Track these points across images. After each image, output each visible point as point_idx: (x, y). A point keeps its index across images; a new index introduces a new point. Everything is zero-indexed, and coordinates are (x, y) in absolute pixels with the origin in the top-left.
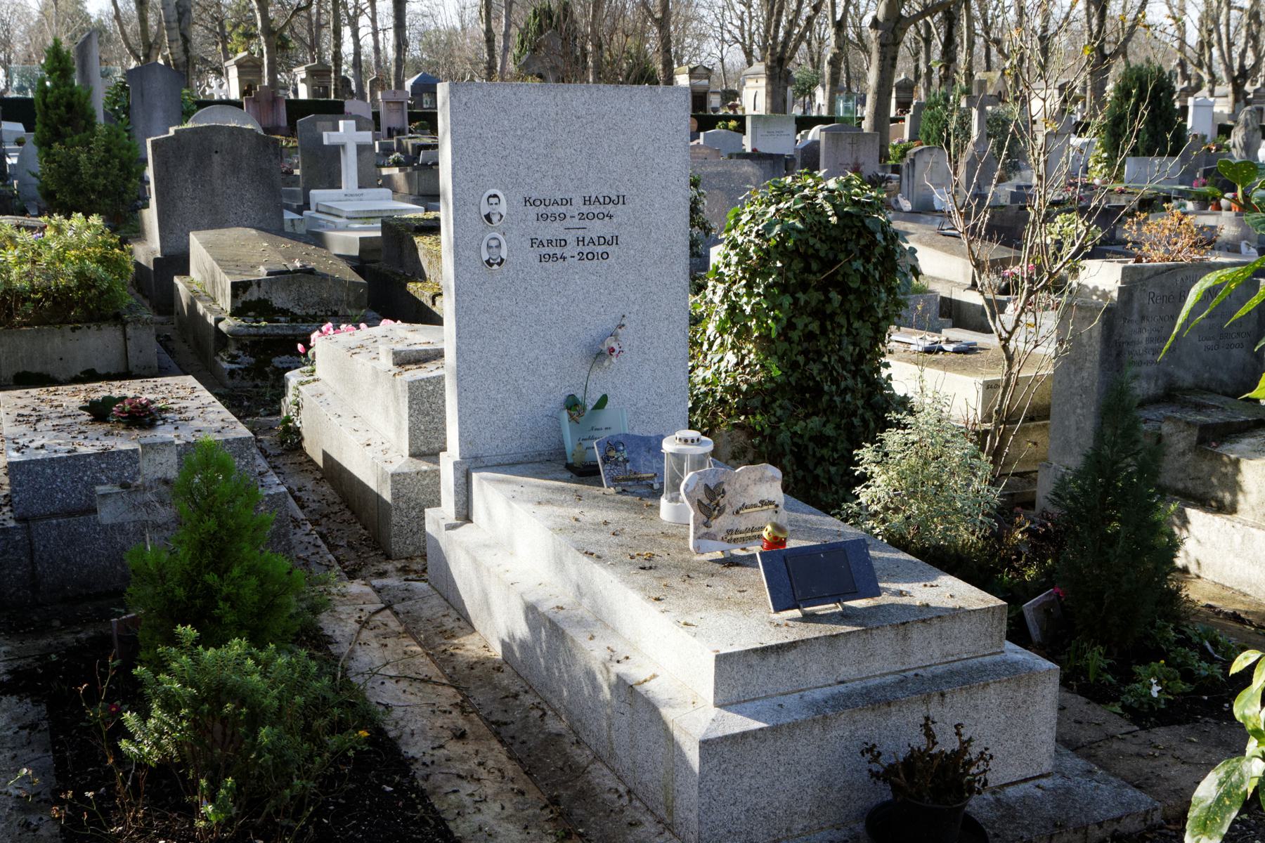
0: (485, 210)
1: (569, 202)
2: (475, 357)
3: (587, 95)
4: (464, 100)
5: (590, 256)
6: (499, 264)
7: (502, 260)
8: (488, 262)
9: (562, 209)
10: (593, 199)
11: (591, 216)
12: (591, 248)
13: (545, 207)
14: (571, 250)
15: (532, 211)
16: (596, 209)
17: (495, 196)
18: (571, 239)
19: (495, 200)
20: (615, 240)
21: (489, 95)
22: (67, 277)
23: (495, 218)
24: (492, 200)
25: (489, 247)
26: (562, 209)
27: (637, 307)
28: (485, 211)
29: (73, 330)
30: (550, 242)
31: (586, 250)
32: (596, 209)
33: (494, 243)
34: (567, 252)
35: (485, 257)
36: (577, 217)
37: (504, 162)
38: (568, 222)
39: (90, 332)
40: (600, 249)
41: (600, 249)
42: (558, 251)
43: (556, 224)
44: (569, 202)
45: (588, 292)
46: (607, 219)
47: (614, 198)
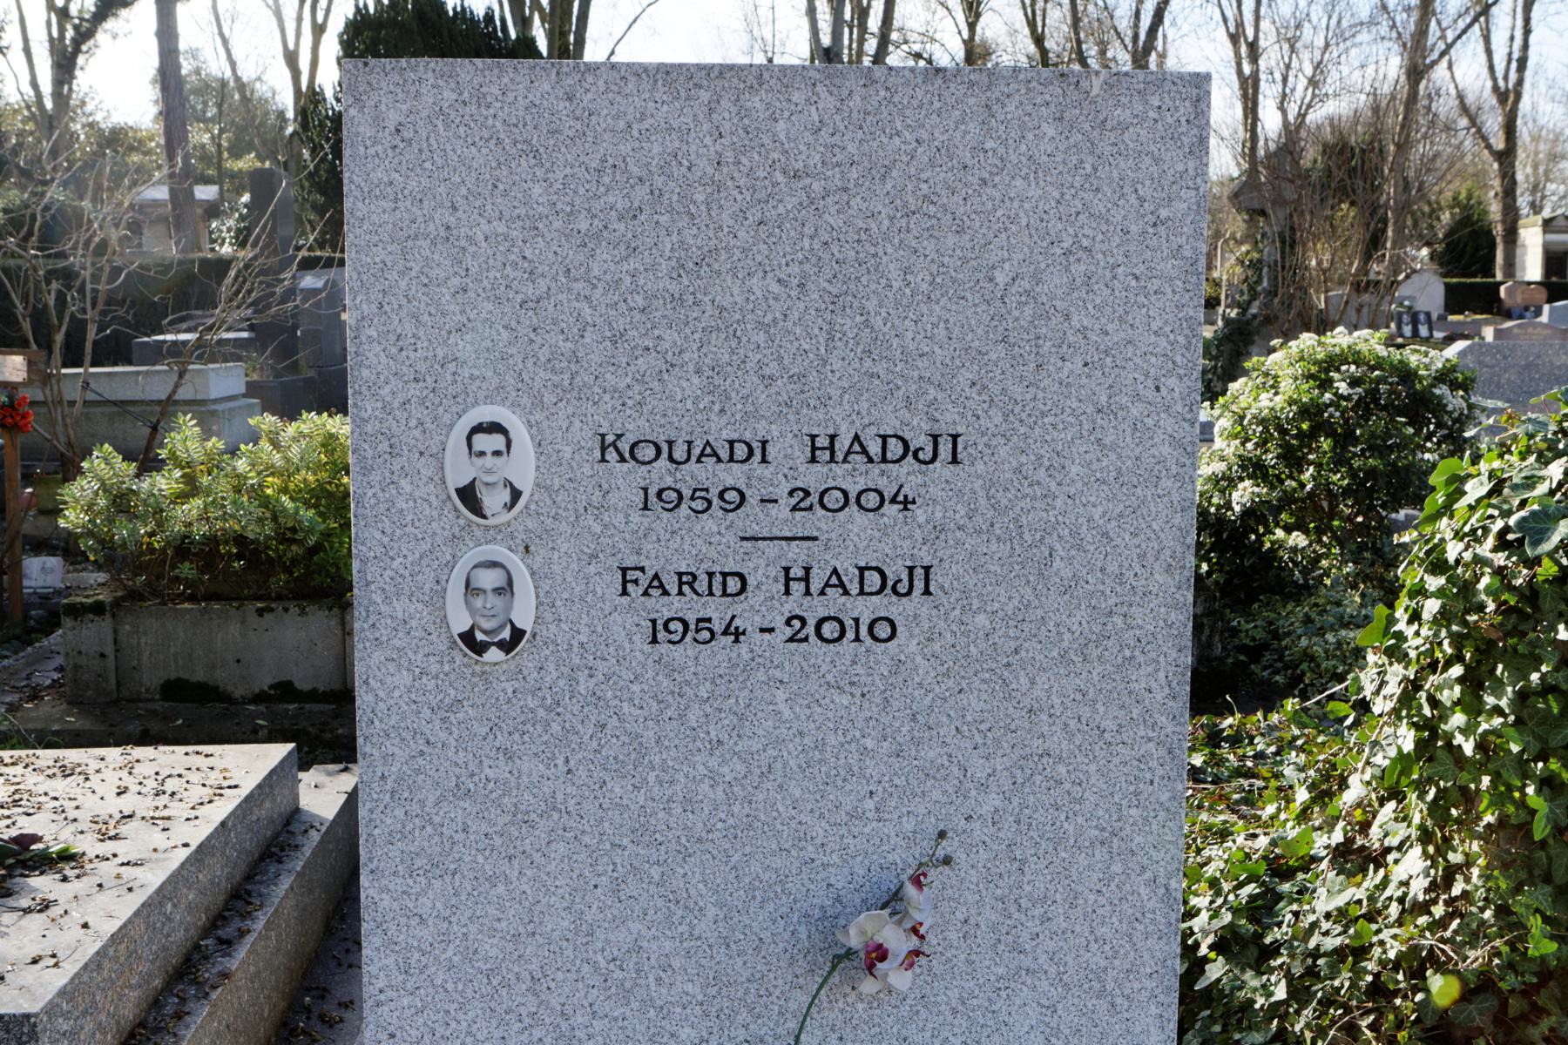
0: (460, 471)
1: (759, 451)
2: (426, 934)
3: (828, 101)
4: (393, 118)
5: (829, 630)
6: (507, 647)
7: (518, 634)
8: (468, 638)
9: (733, 475)
10: (843, 443)
11: (834, 499)
12: (834, 602)
13: (678, 469)
14: (764, 605)
15: (627, 480)
16: (853, 475)
17: (495, 428)
18: (762, 568)
19: (497, 441)
20: (920, 579)
21: (480, 99)
22: (246, 521)
23: (493, 501)
24: (483, 441)
25: (470, 589)
26: (733, 475)
27: (995, 800)
28: (458, 476)
29: (260, 612)
30: (687, 580)
31: (816, 609)
32: (853, 475)
33: (489, 579)
34: (748, 613)
35: (461, 623)
36: (786, 502)
37: (529, 319)
38: (752, 518)
39: (287, 618)
40: (865, 608)
41: (865, 608)
42: (717, 611)
43: (708, 523)
44: (759, 451)
45: (820, 745)
46: (891, 510)
47: (920, 440)
